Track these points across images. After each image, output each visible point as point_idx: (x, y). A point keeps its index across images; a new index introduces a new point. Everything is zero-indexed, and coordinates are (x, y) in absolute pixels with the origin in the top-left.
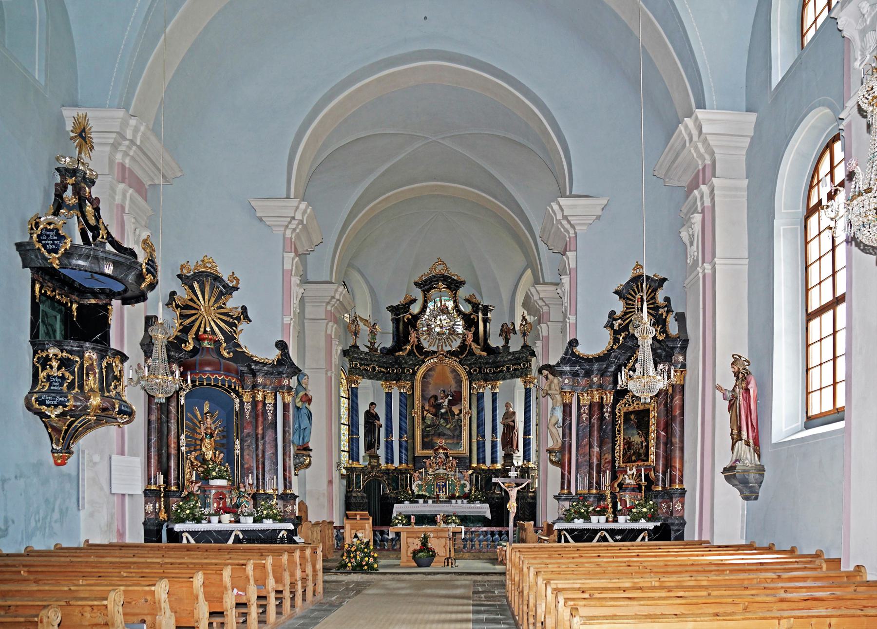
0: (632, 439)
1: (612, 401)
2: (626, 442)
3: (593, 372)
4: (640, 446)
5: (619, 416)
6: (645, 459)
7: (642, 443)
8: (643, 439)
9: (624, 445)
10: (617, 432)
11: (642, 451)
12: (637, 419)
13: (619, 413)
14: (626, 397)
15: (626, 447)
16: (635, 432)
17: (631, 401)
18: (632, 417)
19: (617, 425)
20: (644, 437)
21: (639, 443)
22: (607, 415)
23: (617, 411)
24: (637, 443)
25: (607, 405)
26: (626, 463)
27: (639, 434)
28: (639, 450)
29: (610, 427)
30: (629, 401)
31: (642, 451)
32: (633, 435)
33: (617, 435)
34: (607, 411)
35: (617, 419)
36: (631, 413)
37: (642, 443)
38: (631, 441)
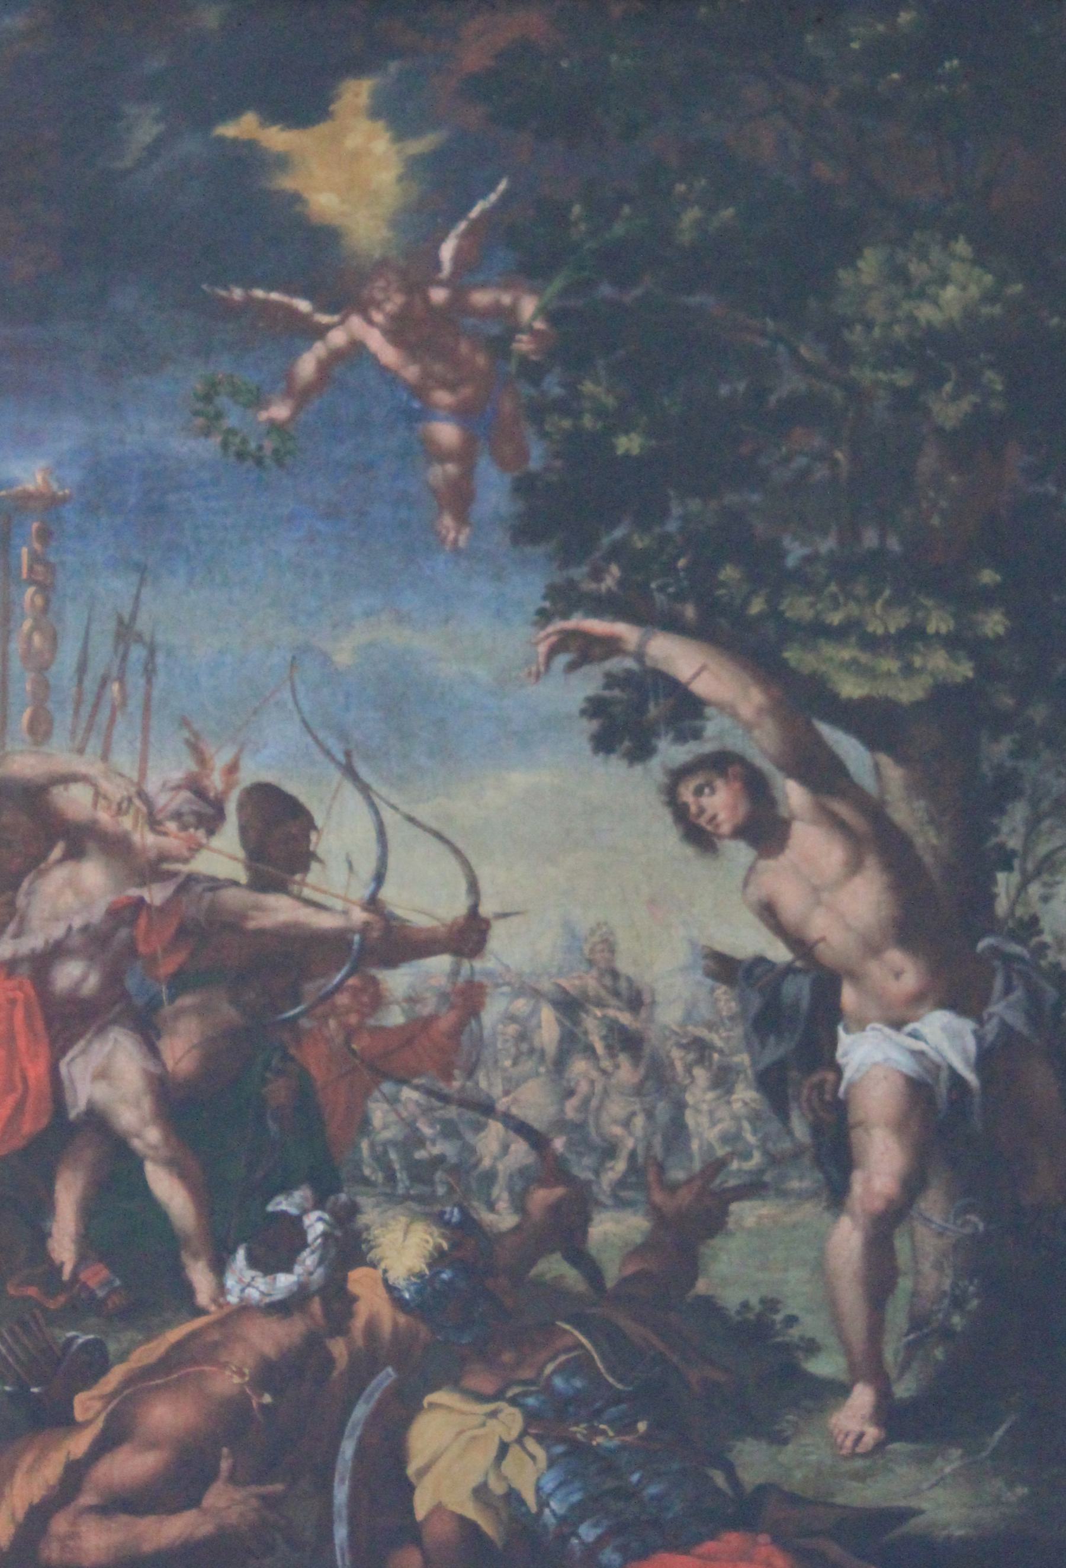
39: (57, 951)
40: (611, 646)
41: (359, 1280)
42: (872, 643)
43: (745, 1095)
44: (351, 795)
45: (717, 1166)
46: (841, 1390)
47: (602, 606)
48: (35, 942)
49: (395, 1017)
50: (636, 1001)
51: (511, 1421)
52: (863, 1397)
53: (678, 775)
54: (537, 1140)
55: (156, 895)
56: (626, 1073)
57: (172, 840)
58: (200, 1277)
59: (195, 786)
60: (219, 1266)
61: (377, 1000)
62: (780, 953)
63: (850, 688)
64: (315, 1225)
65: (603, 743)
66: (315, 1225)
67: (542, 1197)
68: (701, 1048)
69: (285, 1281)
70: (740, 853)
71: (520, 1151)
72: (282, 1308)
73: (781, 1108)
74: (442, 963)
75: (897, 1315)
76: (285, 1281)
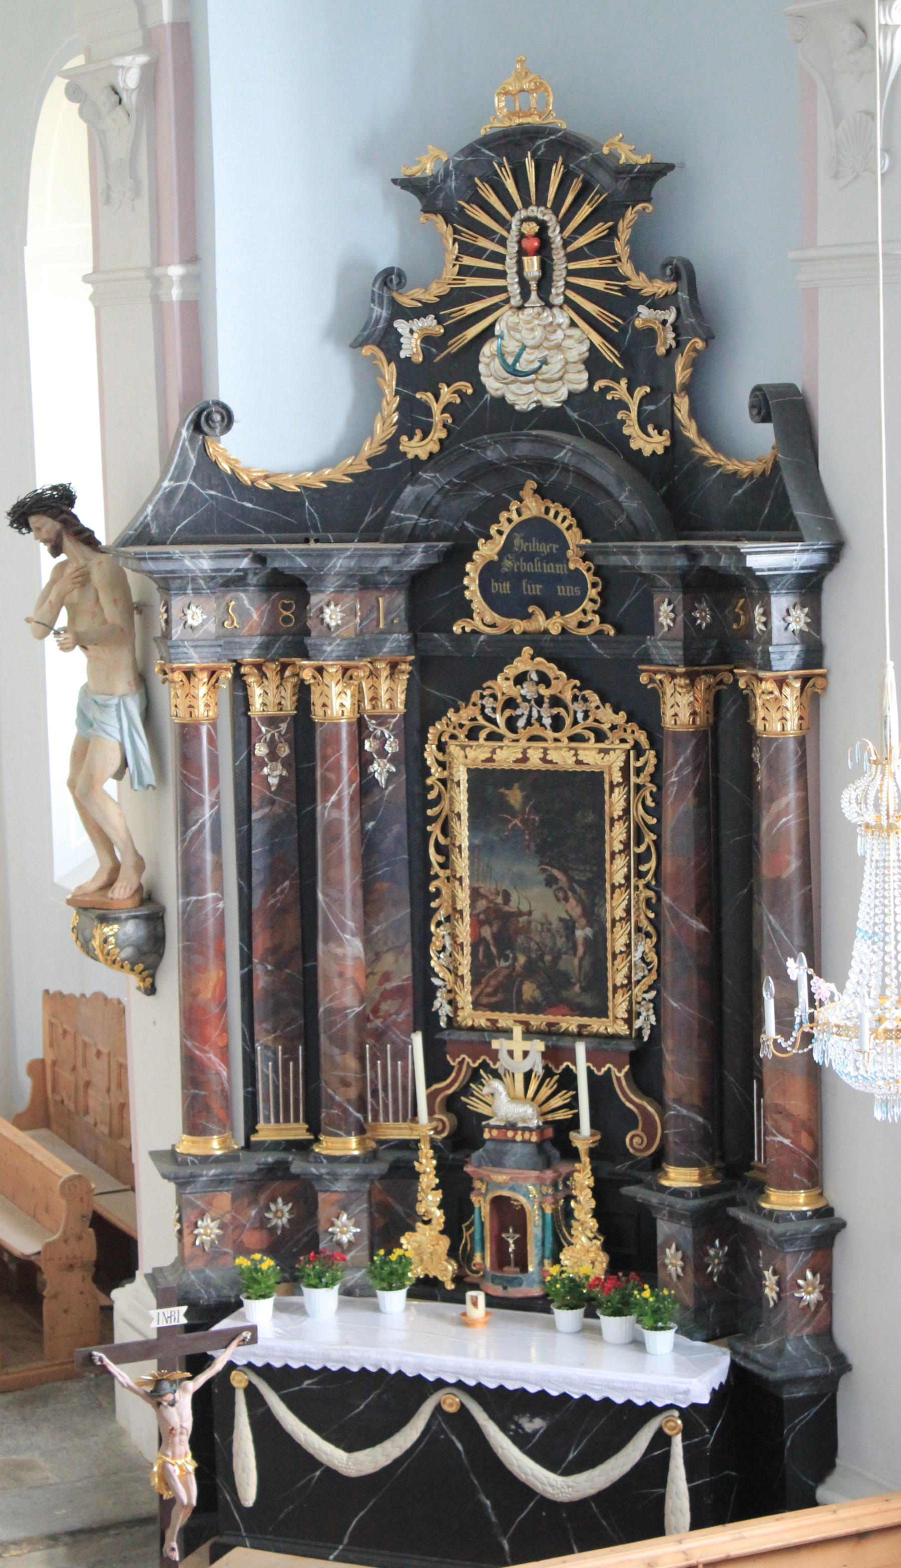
0: (518, 902)
1: (401, 707)
2: (486, 911)
3: (320, 579)
4: (560, 942)
5: (443, 781)
6: (588, 1001)
7: (569, 926)
8: (574, 909)
9: (477, 923)
10: (434, 857)
11: (571, 964)
12: (536, 809)
13: (442, 765)
14: (475, 696)
15: (486, 932)
16: (531, 868)
17: (500, 719)
18: (515, 796)
19: (433, 820)
20: (580, 901)
21: (556, 924)
22: (380, 769)
23: (431, 753)
24: (545, 924)
25: (382, 720)
26: (493, 1007)
27: (550, 881)
28: (557, 958)
29: (398, 828)
30: (493, 722)
31: (571, 964)
32: (520, 881)
33: (436, 869)
34: (382, 753)
35: (432, 796)
36: (508, 777)
37: (569, 926)
38: (512, 907)
39: (479, 914)
40: (547, 870)
41: (516, 964)
42: (580, 871)
43: (564, 939)
44: (515, 892)
45: (560, 950)
46: (575, 984)
47: (546, 864)
48: (477, 912)
49: (520, 925)
50: (550, 924)
51: (534, 986)
52: (578, 986)
53: (556, 890)
54: (538, 944)
55: (492, 905)
56: (549, 935)
57: (492, 897)
58: (497, 962)
59: (496, 889)
60: (499, 961)
61: (518, 922)
62: (568, 918)
63: (577, 878)
64: (511, 955)
65: (546, 885)
66: (511, 955)
67: (539, 953)
68: (558, 931)
69: (507, 964)
70: (563, 902)
71: (536, 946)
72: (507, 968)
73: (568, 942)
74: (526, 917)
75: (582, 973)
76: (507, 964)
